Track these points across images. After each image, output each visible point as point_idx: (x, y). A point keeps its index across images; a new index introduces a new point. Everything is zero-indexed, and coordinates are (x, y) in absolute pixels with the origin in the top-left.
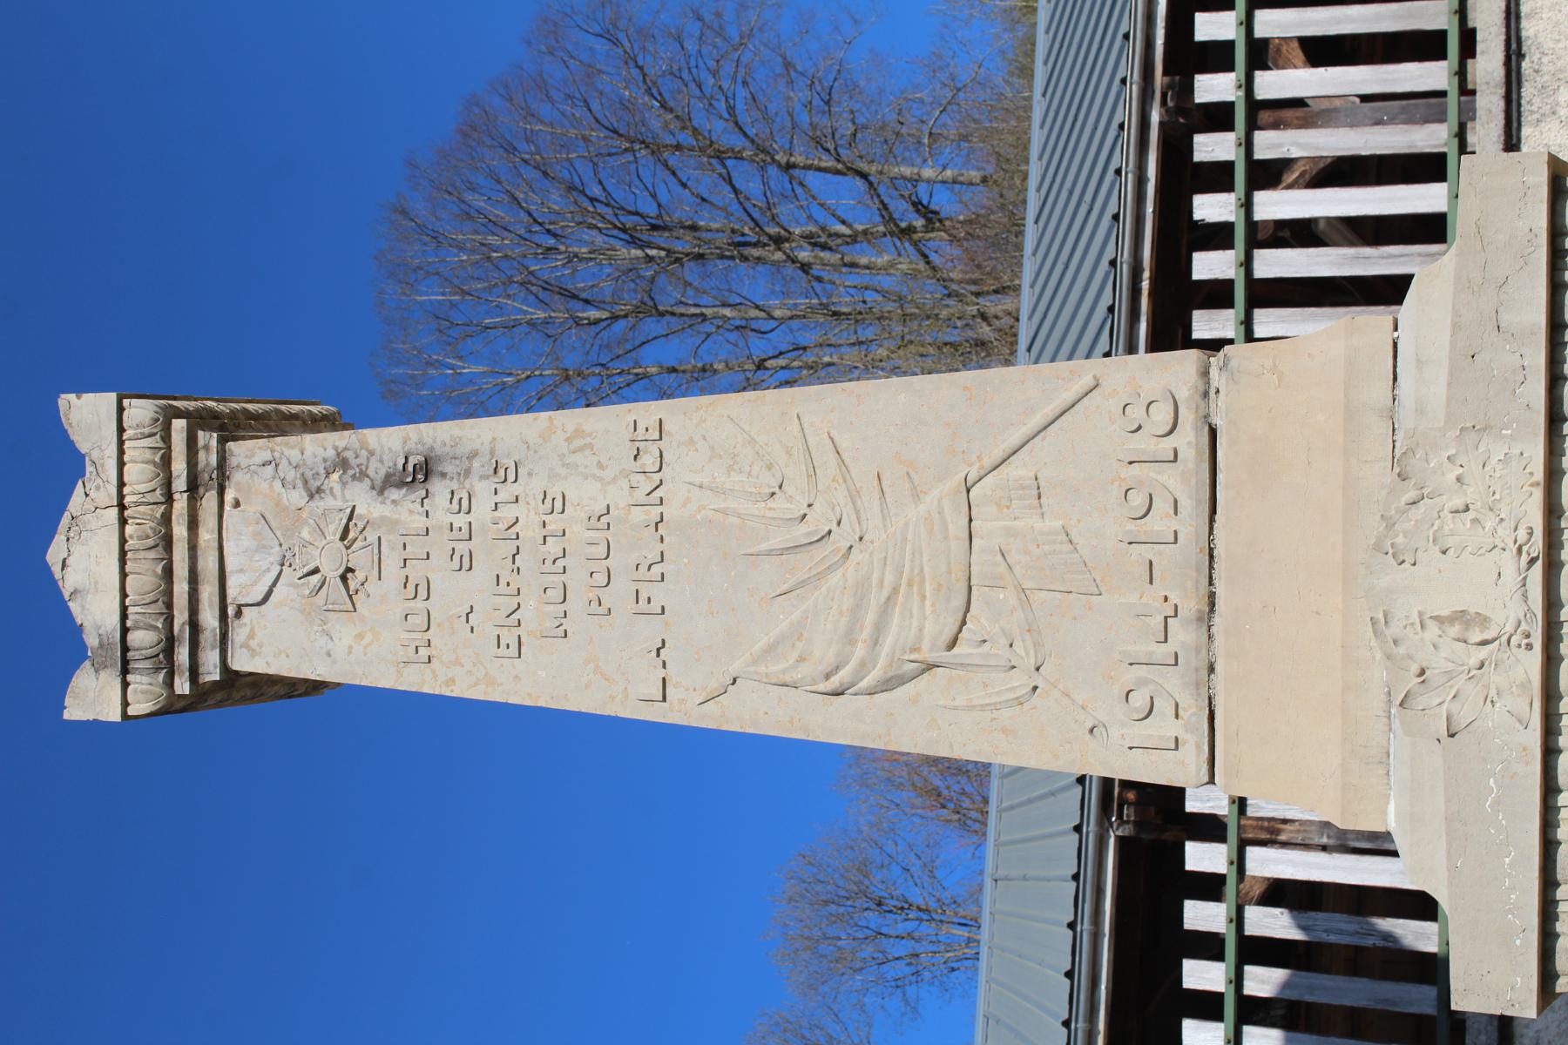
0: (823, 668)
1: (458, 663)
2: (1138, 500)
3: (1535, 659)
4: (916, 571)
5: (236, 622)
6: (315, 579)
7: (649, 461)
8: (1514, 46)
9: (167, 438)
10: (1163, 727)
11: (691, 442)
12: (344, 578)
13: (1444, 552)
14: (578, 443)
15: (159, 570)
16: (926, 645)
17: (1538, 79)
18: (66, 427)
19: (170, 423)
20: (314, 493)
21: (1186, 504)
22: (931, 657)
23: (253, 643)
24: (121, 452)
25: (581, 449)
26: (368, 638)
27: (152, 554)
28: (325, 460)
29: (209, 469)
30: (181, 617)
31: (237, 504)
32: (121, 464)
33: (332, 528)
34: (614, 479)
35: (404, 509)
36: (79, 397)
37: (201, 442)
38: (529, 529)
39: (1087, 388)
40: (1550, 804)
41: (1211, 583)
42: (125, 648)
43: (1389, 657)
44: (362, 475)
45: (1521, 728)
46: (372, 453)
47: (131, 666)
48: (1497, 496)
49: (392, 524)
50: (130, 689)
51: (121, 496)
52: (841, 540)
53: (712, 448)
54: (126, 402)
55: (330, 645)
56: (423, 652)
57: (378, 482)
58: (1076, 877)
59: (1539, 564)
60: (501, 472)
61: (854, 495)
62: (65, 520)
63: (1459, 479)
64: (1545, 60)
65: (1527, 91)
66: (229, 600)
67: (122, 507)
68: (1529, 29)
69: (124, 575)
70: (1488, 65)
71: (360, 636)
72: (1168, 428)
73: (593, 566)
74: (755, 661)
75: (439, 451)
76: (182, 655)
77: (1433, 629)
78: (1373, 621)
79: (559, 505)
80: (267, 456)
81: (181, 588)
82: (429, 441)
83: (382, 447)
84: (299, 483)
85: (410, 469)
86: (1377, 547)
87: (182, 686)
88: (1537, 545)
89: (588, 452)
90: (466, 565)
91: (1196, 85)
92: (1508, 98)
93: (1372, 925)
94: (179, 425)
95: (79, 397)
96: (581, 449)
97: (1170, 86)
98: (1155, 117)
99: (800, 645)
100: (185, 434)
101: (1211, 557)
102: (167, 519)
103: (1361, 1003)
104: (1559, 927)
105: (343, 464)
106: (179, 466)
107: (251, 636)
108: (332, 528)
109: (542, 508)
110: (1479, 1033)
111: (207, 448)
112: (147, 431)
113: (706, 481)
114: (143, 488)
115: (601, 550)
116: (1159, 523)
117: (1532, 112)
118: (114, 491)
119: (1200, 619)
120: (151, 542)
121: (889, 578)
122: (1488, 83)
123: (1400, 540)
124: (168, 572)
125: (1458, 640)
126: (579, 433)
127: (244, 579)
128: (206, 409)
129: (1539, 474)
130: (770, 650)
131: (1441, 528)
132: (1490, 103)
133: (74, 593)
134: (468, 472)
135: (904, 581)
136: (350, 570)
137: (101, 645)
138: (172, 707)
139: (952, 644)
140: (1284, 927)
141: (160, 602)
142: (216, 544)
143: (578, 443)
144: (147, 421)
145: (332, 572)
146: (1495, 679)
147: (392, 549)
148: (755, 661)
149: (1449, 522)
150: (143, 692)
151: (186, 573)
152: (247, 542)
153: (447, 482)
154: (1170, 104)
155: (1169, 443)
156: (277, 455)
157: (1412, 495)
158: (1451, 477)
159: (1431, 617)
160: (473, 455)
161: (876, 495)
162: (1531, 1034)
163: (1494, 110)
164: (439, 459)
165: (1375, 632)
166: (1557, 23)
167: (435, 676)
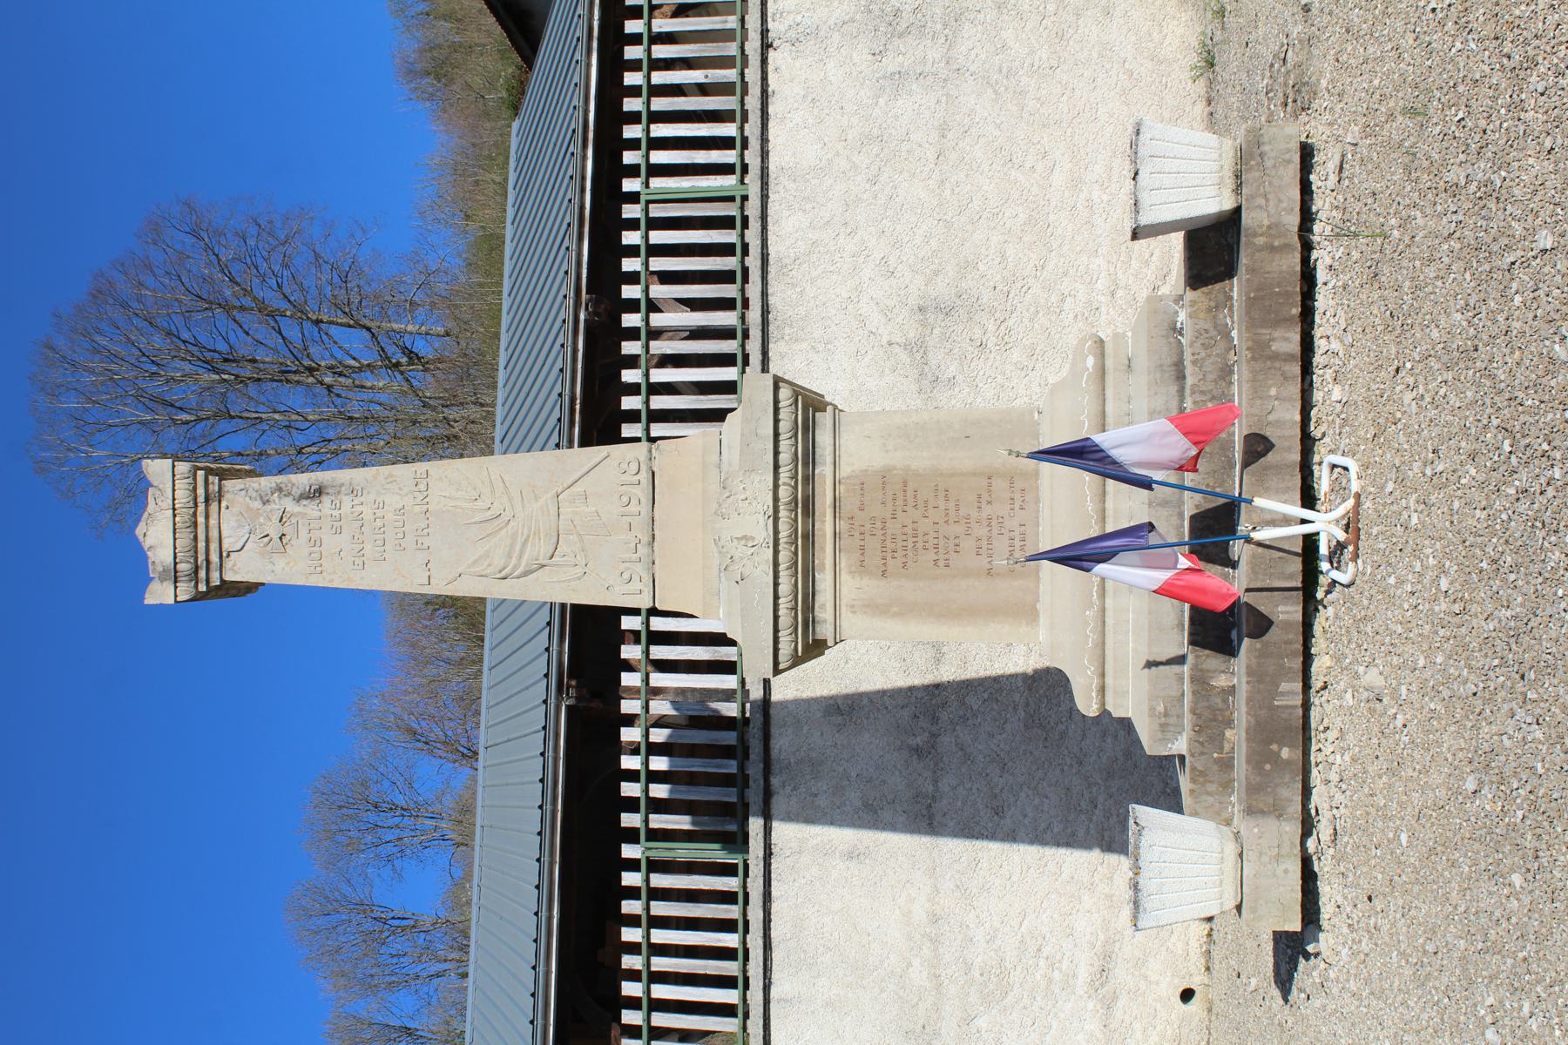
0: (499, 568)
1: (334, 572)
2: (625, 499)
6: (266, 539)
7: (422, 487)
9: (195, 479)
10: (636, 585)
11: (441, 479)
12: (281, 538)
14: (390, 480)
15: (192, 536)
16: (541, 558)
22: (542, 561)
23: (235, 568)
24: (174, 485)
25: (391, 482)
26: (291, 565)
27: (189, 530)
30: (201, 558)
32: (174, 490)
35: (310, 508)
37: (210, 481)
38: (368, 513)
42: (176, 572)
43: (720, 552)
44: (289, 494)
46: (294, 485)
49: (303, 515)
51: (174, 505)
52: (505, 518)
54: (176, 463)
55: (274, 568)
57: (297, 496)
61: (510, 499)
62: (145, 516)
67: (174, 509)
68: (772, 300)
69: (175, 539)
70: (754, 315)
71: (288, 563)
75: (325, 483)
76: (202, 574)
77: (735, 541)
79: (381, 505)
80: (242, 486)
81: (201, 545)
82: (321, 480)
84: (258, 498)
86: (715, 513)
87: (202, 588)
88: (771, 512)
94: (201, 473)
96: (391, 482)
97: (590, 300)
98: (582, 317)
99: (488, 560)
102: (195, 514)
105: (280, 490)
106: (201, 491)
111: (213, 483)
113: (447, 494)
114: (184, 501)
115: (401, 524)
116: (633, 508)
120: (188, 525)
121: (526, 532)
124: (196, 538)
126: (390, 475)
127: (231, 540)
129: (771, 487)
130: (475, 562)
132: (755, 333)
134: (339, 492)
136: (284, 535)
137: (164, 571)
138: (198, 597)
139: (552, 557)
143: (390, 480)
145: (275, 536)
147: (303, 525)
152: (233, 524)
154: (590, 309)
155: (637, 477)
157: (727, 494)
160: (343, 485)
164: (326, 487)
166: (783, 299)
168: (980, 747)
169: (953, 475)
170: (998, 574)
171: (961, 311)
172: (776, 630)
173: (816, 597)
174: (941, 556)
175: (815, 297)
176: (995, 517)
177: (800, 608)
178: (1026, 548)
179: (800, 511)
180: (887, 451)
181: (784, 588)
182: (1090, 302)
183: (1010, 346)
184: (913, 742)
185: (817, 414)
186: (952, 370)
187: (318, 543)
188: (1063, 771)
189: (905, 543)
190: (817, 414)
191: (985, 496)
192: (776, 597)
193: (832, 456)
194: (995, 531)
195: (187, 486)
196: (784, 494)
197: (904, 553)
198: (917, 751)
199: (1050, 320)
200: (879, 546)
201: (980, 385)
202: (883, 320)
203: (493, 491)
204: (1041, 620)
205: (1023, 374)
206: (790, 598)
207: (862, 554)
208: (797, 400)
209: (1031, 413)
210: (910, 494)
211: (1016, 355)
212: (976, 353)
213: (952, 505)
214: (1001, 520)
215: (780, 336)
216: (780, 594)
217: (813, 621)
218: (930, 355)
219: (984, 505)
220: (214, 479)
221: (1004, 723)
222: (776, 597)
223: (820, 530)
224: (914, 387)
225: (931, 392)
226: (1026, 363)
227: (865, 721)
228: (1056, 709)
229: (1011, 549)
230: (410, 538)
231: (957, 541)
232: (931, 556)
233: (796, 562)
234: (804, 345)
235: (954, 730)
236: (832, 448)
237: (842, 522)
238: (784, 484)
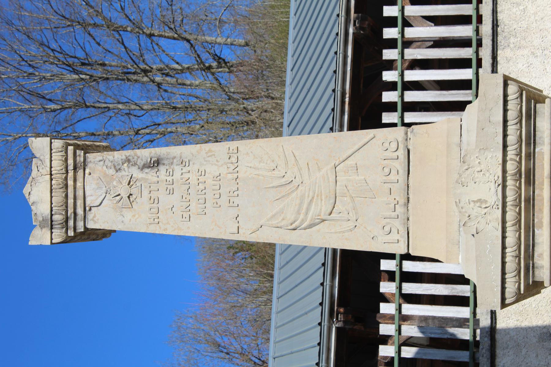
0: (290, 222)
1: (168, 223)
2: (387, 170)
3: (500, 212)
4: (320, 192)
5: (89, 212)
6: (118, 198)
7: (234, 160)
8: (495, 22)
9: (66, 152)
10: (394, 236)
11: (247, 153)
13: (475, 183)
14: (210, 154)
15: (64, 195)
16: (322, 214)
17: (503, 34)
18: (31, 148)
19: (68, 147)
20: (118, 170)
21: (401, 172)
23: (95, 219)
24: (51, 157)
25: (211, 156)
26: (137, 216)
27: (62, 190)
28: (122, 160)
29: (80, 162)
30: (71, 211)
31: (90, 174)
32: (51, 161)
33: (125, 181)
34: (222, 165)
35: (150, 175)
36: (36, 139)
37: (78, 154)
38: (193, 180)
39: (371, 138)
40: (504, 252)
41: (408, 194)
42: (52, 221)
43: (460, 212)
44: (135, 164)
45: (496, 231)
46: (139, 157)
47: (54, 226)
48: (489, 167)
49: (146, 180)
50: (53, 234)
51: (51, 171)
52: (295, 183)
53: (254, 155)
54: (53, 141)
55: (123, 219)
56: (156, 220)
57: (141, 166)
58: (319, 344)
59: (501, 186)
60: (184, 163)
61: (300, 170)
62: (30, 179)
63: (479, 163)
64: (506, 27)
65: (500, 38)
66: (87, 205)
67: (51, 175)
68: (500, 16)
69: (51, 197)
70: (486, 28)
71: (134, 216)
72: (396, 149)
73: (215, 192)
74: (268, 220)
75: (162, 156)
76: (71, 223)
77: (472, 204)
78: (456, 202)
79: (203, 173)
80: (101, 158)
81: (71, 201)
83: (142, 155)
84: (113, 167)
85: (152, 162)
86: (457, 182)
87: (71, 233)
88: (500, 180)
89: (213, 157)
90: (171, 192)
91: (384, 32)
92: (493, 41)
93: (447, 330)
94: (71, 148)
95: (36, 139)
96: (211, 156)
97: (357, 18)
98: (351, 31)
100: (73, 151)
101: (408, 187)
102: (66, 178)
103: (443, 359)
104: (506, 285)
105: (129, 161)
106: (71, 162)
107: (95, 216)
108: (125, 181)
109: (197, 174)
110: (484, 365)
111: (80, 156)
112: (60, 150)
113: (252, 166)
114: (59, 168)
115: (218, 187)
116: (393, 177)
117: (501, 46)
118: (49, 170)
119: (405, 205)
120: (61, 186)
121: (311, 194)
122: (486, 35)
123: (463, 180)
124: (67, 196)
125: (479, 207)
126: (210, 151)
127: (92, 198)
128: (75, 143)
129: (501, 162)
130: (273, 216)
131: (474, 176)
132: (487, 42)
133: (33, 203)
134: (172, 163)
135: (316, 195)
136: (131, 195)
137: (43, 220)
138: (68, 240)
140: (415, 332)
141: (64, 206)
142: (83, 187)
143: (210, 154)
144: (60, 147)
145: (125, 195)
146: (489, 217)
147: (146, 187)
148: (268, 220)
149: (477, 175)
150: (57, 235)
151: (73, 196)
153: (165, 166)
154: (357, 25)
156: (104, 158)
157: (466, 167)
158: (477, 162)
159: (472, 201)
160: (174, 158)
161: (307, 169)
162: (502, 364)
163: (488, 45)
164: (162, 159)
165: (456, 205)
166: (510, 15)
167: (160, 228)
172: (503, 273)
173: (536, 248)
175: (535, 14)
177: (522, 256)
179: (523, 180)
181: (511, 240)
185: (538, 106)
187: (156, 201)
190: (538, 106)
192: (504, 247)
195: (60, 158)
196: (511, 167)
203: (287, 163)
206: (515, 248)
208: (521, 95)
215: (506, 44)
216: (507, 245)
217: (533, 267)
220: (80, 153)
222: (504, 247)
223: (538, 196)
230: (224, 198)
233: (520, 221)
234: (526, 52)
238: (511, 159)
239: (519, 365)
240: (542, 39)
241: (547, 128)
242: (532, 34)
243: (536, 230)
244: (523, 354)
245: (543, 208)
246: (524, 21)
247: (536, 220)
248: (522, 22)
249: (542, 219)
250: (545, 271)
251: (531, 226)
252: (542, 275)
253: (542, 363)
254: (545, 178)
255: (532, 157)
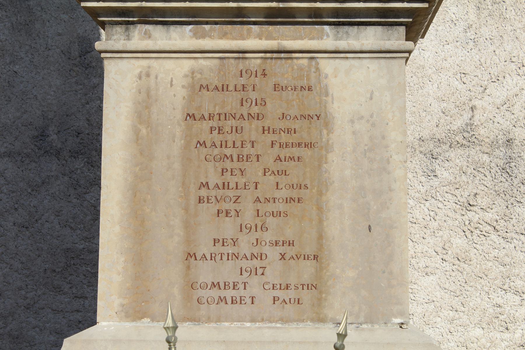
168: (46, 201)
169: (320, 209)
170: (188, 268)
171: (506, 185)
173: (159, 27)
174: (213, 193)
176: (264, 263)
178: (222, 304)
180: (352, 121)
182: (514, 321)
183: (469, 236)
184: (52, 130)
185: (402, 30)
186: (444, 174)
188: (20, 288)
189: (230, 144)
190: (402, 30)
191: (290, 251)
193: (347, 48)
194: (245, 264)
197: (218, 144)
198: (42, 135)
199: (496, 279)
200: (228, 109)
201: (427, 204)
202: (498, 102)
204: (128, 325)
205: (439, 250)
207: (217, 88)
209: (401, 314)
210: (296, 152)
211: (459, 242)
212: (461, 200)
213: (281, 207)
214: (260, 271)
217: (128, 23)
218: (460, 151)
219: (280, 249)
221: (71, 228)
223: (249, 32)
224: (426, 134)
225: (421, 152)
226: (450, 252)
227: (74, 80)
228: (85, 282)
229: (222, 285)
231: (233, 213)
232: (214, 179)
234: (472, 17)
235: (64, 175)
236: (358, 48)
237: (259, 61)
239: (47, 10)
240: (489, 39)
241: (363, 44)
242: (496, 26)
243: (190, 27)
244: (62, 15)
245: (228, 39)
246: (514, 14)
247: (207, 27)
248: (513, 11)
249: (210, 37)
250: (122, 42)
251: (197, 19)
252: (115, 37)
253: (50, 41)
254: (279, 41)
255: (314, 20)
